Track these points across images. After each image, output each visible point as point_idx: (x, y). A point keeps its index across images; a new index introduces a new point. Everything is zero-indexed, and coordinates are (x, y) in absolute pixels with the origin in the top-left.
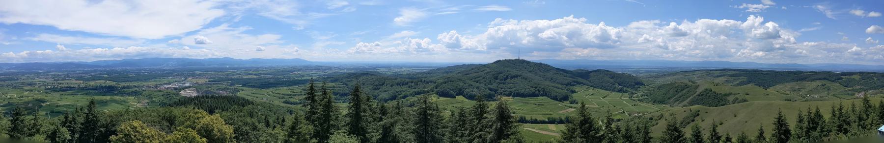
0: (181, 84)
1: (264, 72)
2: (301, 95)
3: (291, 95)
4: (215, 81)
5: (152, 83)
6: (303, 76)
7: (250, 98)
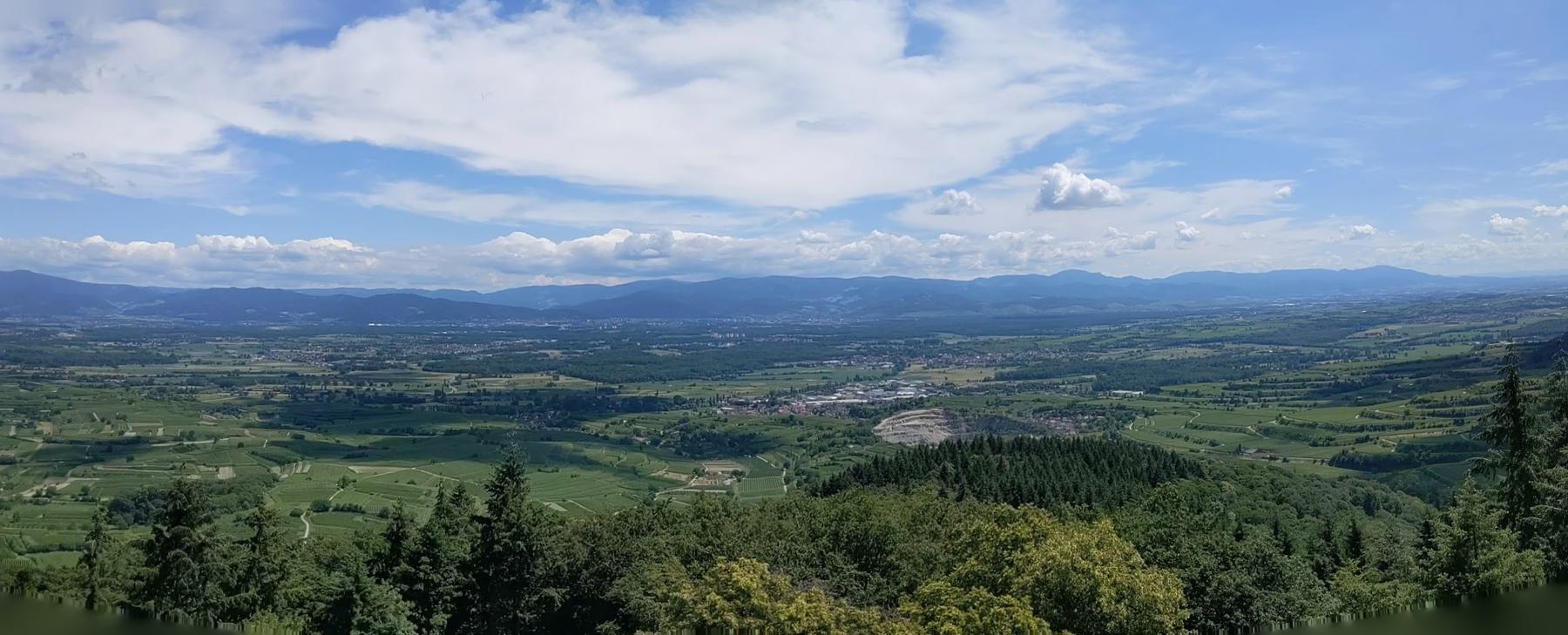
0: (880, 392)
1: (1240, 330)
2: (1411, 426)
3: (1362, 429)
4: (1027, 378)
5: (752, 388)
6: (1413, 343)
7: (1180, 447)
